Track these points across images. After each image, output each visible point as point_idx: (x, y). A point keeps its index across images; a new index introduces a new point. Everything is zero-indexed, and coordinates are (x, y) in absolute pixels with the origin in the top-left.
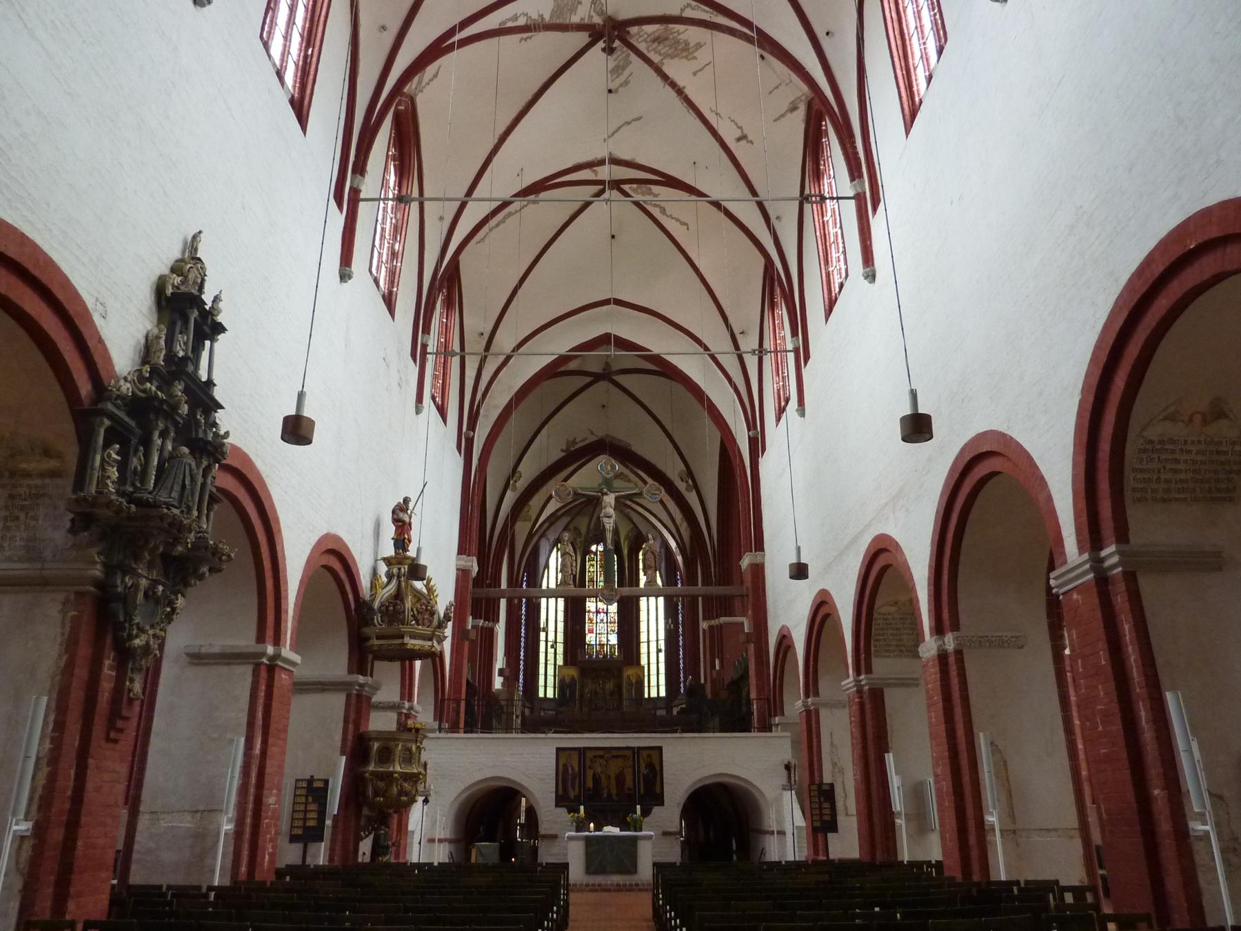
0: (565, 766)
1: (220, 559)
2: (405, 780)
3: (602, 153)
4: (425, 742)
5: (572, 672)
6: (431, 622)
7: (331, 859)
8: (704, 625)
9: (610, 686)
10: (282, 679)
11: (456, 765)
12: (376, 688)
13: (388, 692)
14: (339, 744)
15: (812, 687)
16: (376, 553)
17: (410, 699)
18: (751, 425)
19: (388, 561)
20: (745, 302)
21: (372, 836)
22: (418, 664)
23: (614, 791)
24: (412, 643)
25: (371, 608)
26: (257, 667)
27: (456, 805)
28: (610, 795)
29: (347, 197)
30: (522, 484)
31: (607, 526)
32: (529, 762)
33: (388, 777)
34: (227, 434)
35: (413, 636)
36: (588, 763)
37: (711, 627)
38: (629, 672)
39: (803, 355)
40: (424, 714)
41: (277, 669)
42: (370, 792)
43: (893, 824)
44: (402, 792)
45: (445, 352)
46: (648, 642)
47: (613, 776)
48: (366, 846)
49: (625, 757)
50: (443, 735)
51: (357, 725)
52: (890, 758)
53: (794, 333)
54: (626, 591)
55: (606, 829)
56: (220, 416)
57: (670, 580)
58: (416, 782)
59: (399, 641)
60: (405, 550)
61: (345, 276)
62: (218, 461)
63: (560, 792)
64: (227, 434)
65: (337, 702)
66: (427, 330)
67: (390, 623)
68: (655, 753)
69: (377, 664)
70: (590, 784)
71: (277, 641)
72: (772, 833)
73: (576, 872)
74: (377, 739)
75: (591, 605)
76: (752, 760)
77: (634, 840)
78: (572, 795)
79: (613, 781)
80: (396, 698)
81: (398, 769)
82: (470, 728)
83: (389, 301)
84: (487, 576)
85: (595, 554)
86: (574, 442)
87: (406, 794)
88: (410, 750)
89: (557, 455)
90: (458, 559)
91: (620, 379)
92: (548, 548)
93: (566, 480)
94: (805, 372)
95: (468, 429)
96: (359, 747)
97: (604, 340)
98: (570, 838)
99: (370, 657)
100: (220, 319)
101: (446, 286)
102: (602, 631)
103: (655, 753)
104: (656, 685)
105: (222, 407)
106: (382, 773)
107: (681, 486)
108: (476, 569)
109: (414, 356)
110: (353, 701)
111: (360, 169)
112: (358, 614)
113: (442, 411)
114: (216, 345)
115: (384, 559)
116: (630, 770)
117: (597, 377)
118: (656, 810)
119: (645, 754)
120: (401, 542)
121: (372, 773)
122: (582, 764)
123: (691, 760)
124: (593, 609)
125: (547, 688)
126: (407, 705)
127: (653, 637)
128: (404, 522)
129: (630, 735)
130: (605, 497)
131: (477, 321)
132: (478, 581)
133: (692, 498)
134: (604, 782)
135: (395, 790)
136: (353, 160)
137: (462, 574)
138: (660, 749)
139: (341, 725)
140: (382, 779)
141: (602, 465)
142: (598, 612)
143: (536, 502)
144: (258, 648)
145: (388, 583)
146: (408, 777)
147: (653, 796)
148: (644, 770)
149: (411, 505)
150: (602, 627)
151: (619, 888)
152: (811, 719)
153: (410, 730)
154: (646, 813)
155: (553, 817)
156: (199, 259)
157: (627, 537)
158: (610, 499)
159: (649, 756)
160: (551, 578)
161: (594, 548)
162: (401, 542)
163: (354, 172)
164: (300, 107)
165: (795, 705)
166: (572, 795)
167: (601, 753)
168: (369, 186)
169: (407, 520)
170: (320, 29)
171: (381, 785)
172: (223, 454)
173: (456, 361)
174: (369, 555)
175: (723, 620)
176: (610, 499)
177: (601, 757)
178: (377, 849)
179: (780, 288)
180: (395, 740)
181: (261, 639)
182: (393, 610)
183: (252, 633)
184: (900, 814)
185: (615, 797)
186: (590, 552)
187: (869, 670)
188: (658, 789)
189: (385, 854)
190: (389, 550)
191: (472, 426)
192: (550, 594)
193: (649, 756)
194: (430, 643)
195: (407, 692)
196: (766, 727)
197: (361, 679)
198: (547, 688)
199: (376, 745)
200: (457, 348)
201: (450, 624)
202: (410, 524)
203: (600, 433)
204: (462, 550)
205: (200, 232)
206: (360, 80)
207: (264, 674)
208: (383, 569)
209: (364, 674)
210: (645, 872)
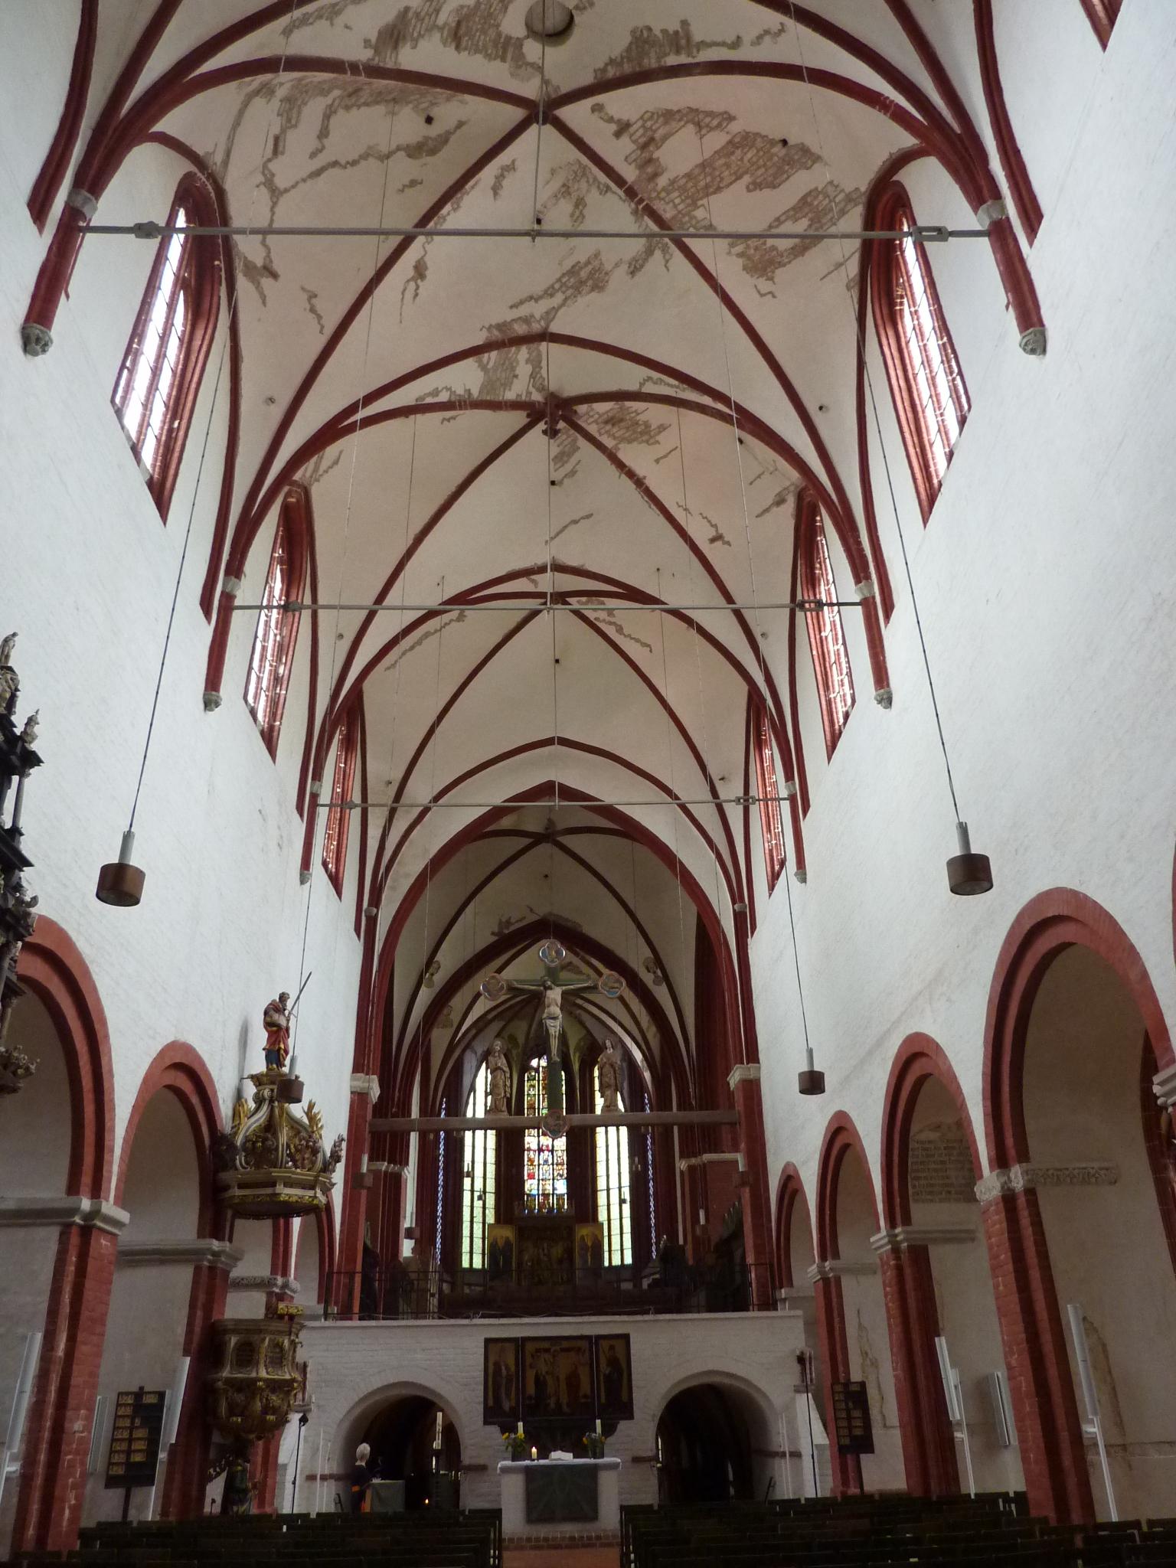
0: (497, 1365)
1: (15, 1073)
2: (273, 1391)
3: (543, 558)
4: (303, 1335)
5: (507, 1233)
6: (313, 1163)
7: (164, 1513)
8: (681, 1165)
9: (558, 1251)
10: (102, 1245)
11: (348, 1365)
12: (236, 1259)
13: (254, 1263)
14: (182, 1340)
15: (829, 1247)
16: (241, 1069)
17: (285, 1273)
18: (736, 896)
19: (257, 1079)
20: (724, 736)
21: (224, 1475)
22: (297, 1222)
24: (287, 1193)
25: (232, 1146)
26: (66, 1229)
27: (346, 1425)
28: (558, 1404)
29: (217, 604)
30: (440, 978)
31: (552, 1031)
32: (444, 1359)
33: (248, 1387)
34: (35, 900)
35: (289, 1184)
36: (529, 1360)
37: (692, 1169)
38: (583, 1231)
39: (801, 803)
40: (304, 1294)
41: (95, 1233)
42: (223, 1409)
43: (952, 1439)
44: (267, 1409)
45: (342, 803)
46: (608, 1190)
47: (562, 1377)
48: (215, 1490)
49: (579, 1349)
50: (329, 1323)
51: (208, 1309)
52: (941, 1344)
53: (789, 777)
54: (578, 1119)
56: (26, 875)
57: (635, 1102)
58: (288, 1393)
59: (269, 1191)
60: (281, 1064)
61: (210, 701)
62: (21, 938)
63: (491, 1403)
64: (35, 900)
65: (182, 1277)
66: (318, 776)
67: (258, 1166)
68: (619, 1345)
69: (239, 1223)
70: (531, 1390)
71: (96, 1192)
72: (783, 1455)
73: (513, 1521)
74: (235, 1331)
75: (531, 1140)
76: (752, 1350)
77: (593, 1472)
78: (506, 1406)
79: (563, 1386)
80: (264, 1271)
81: (263, 1374)
82: (368, 1311)
83: (270, 738)
84: (392, 1103)
85: (537, 1070)
86: (508, 923)
87: (274, 1410)
88: (280, 1346)
89: (485, 939)
90: (353, 1079)
91: (567, 840)
92: (474, 1063)
93: (499, 971)
94: (805, 825)
95: (370, 905)
96: (209, 1343)
97: (546, 790)
98: (506, 1470)
99: (229, 1213)
100: (34, 747)
101: (345, 719)
102: (546, 1177)
103: (619, 1345)
104: (619, 1250)
105: (29, 864)
106: (242, 1380)
107: (648, 978)
108: (375, 1092)
109: (300, 808)
110: (204, 1279)
111: (236, 569)
112: (214, 1152)
113: (336, 881)
114: (27, 781)
115: (252, 1077)
117: (538, 839)
118: (623, 1426)
119: (605, 1344)
120: (275, 1053)
121: (229, 1382)
122: (520, 1361)
123: (670, 1352)
124: (534, 1146)
125: (473, 1256)
126: (280, 1281)
127: (614, 1184)
128: (279, 1026)
129: (586, 1319)
130: (549, 992)
131: (383, 767)
132: (381, 1109)
133: (662, 994)
135: (258, 1405)
136: (228, 557)
137: (359, 1099)
138: (626, 1338)
139: (185, 1311)
140: (240, 1390)
141: (545, 952)
142: (540, 1150)
143: (458, 1002)
144: (68, 1202)
145: (257, 1110)
146: (276, 1386)
147: (620, 1407)
148: (605, 1369)
149: (289, 1004)
150: (546, 1171)
151: (573, 1543)
152: (830, 1290)
153: (281, 1317)
154: (609, 1430)
155: (480, 1439)
156: (10, 669)
157: (577, 1048)
158: (555, 995)
159: (612, 1348)
160: (478, 1106)
161: (534, 1063)
162: (275, 1053)
163: (227, 573)
164: (160, 491)
165: (807, 1272)
167: (546, 1345)
168: (246, 591)
169: (283, 1022)
170: (190, 397)
171: (240, 1398)
172: (27, 927)
173: (355, 815)
174: (231, 1071)
175: (707, 1157)
176: (555, 995)
177: (547, 1350)
178: (232, 1493)
179: (767, 720)
180: (260, 1331)
181: (73, 1189)
182: (262, 1147)
183: (63, 1181)
184: (959, 1424)
185: (565, 1408)
186: (528, 1068)
187: (907, 1220)
188: (625, 1397)
189: (241, 1502)
190: (258, 1064)
191: (375, 901)
192: (476, 1125)
193: (612, 1348)
194: (311, 1193)
195: (280, 1263)
196: (769, 1303)
197: (215, 1245)
198: (473, 1256)
199: (233, 1340)
200: (357, 798)
201: (340, 1168)
202: (287, 1029)
203: (542, 910)
204: (358, 1067)
205: (14, 635)
206: (239, 462)
207: (75, 1240)
208: (250, 1090)
209: (219, 1237)
210: (609, 1517)
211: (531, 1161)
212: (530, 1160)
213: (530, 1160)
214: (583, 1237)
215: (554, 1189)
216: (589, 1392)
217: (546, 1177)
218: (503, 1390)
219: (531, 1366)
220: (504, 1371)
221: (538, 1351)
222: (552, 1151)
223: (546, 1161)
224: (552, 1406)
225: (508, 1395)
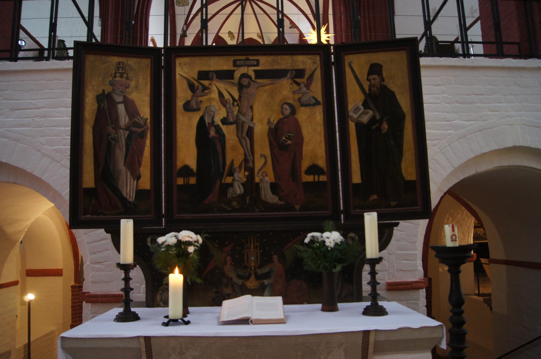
0: (106, 101)
23: (265, 176)
28: (251, 186)
36: (182, 94)
47: (260, 130)
49: (300, 73)
55: (233, 307)
63: (89, 180)
70: (187, 154)
78: (129, 189)
116: (318, 114)
134: (234, 153)
166: (129, 189)
188: (409, 171)
193: (375, 69)
216: (322, 163)
218: (120, 154)
219: (188, 107)
220: (124, 119)
221: (203, 75)
224: (239, 190)
225: (133, 165)
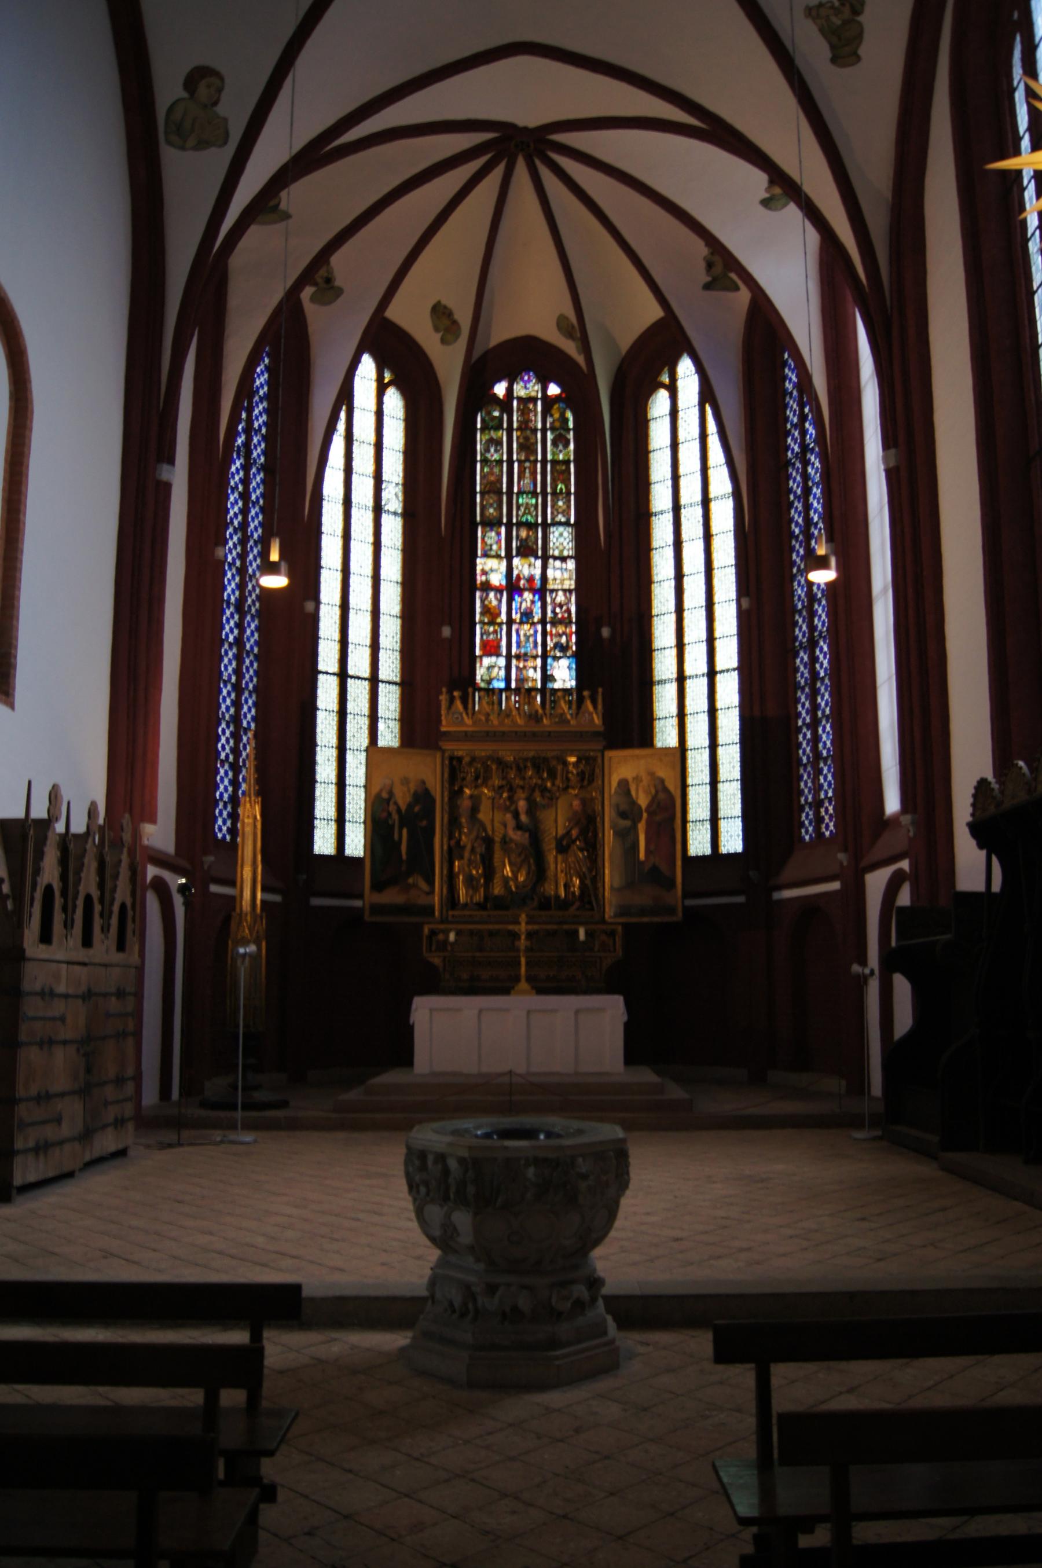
9: (557, 821)
102: (526, 656)
124: (497, 579)
142: (512, 587)
161: (500, 389)
211: (491, 614)
212: (486, 610)
213: (486, 610)
214: (624, 784)
215: (547, 678)
217: (526, 656)
222: (542, 591)
223: (527, 615)
